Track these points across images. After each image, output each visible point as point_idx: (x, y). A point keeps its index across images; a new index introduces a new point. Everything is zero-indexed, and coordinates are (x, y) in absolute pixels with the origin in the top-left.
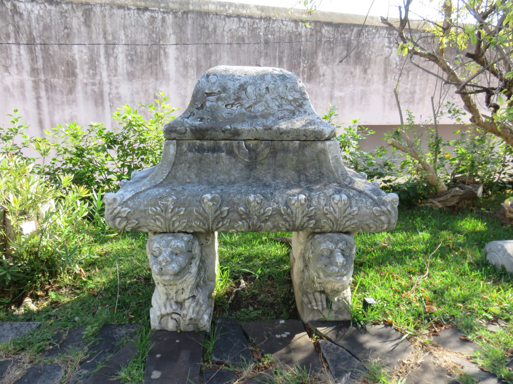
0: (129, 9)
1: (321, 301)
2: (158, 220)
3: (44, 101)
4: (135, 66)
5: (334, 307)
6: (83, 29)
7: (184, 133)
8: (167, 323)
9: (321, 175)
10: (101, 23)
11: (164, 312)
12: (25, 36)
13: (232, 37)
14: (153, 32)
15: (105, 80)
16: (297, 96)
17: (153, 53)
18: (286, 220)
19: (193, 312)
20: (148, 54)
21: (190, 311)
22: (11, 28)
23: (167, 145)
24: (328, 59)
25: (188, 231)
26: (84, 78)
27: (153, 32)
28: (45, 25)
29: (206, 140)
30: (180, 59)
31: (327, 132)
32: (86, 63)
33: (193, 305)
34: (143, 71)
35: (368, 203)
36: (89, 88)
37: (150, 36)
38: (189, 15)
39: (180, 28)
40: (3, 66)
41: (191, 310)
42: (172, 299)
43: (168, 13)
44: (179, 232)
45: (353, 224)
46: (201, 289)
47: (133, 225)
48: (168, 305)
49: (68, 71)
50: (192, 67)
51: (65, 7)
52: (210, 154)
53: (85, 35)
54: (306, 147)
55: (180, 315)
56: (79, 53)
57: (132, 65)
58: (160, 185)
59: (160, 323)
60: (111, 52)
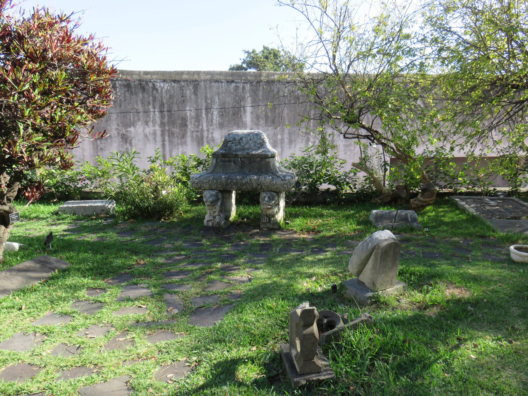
0: (222, 82)
3: (167, 143)
5: (271, 222)
9: (267, 171)
11: (208, 219)
12: (158, 102)
14: (237, 96)
15: (205, 128)
16: (261, 141)
21: (217, 219)
22: (151, 98)
26: (192, 127)
27: (237, 96)
28: (170, 95)
31: (270, 154)
34: (229, 123)
36: (195, 134)
37: (235, 99)
38: (261, 84)
39: (254, 92)
40: (145, 121)
43: (246, 83)
50: (262, 118)
51: (183, 83)
56: (190, 112)
57: (222, 118)
58: (210, 173)
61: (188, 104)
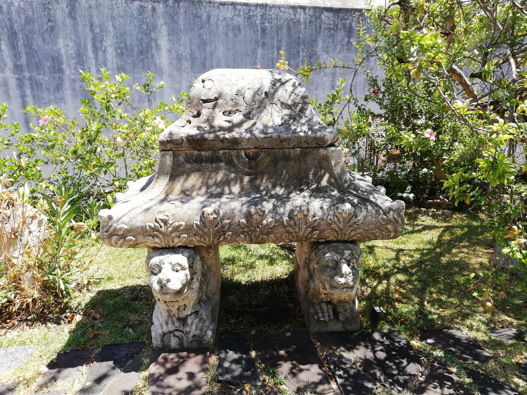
1: (328, 312)
2: (157, 236)
4: (125, 59)
5: (341, 317)
6: (68, 21)
7: (181, 144)
8: (170, 340)
10: (86, 14)
11: (165, 329)
13: (227, 26)
14: (143, 22)
17: (144, 45)
18: (289, 233)
19: (196, 329)
20: (138, 46)
23: (163, 156)
24: (328, 47)
25: (189, 246)
26: (71, 73)
28: (26, 18)
29: (204, 150)
30: (173, 51)
32: (73, 58)
33: (196, 321)
34: (134, 65)
41: (194, 327)
42: (174, 315)
44: (179, 247)
45: (358, 234)
46: (204, 303)
48: (170, 322)
49: (54, 67)
50: (186, 59)
52: (208, 164)
53: (70, 27)
54: (308, 154)
55: (182, 332)
56: (64, 46)
59: (162, 341)
60: (100, 45)
61: (61, 33)
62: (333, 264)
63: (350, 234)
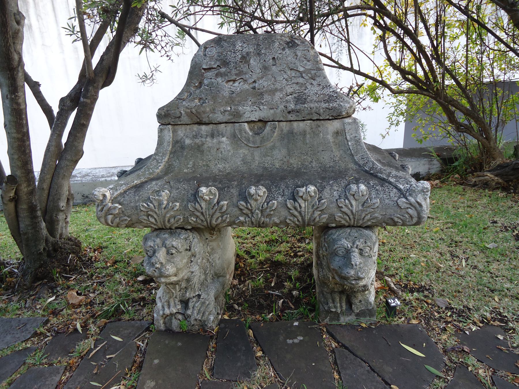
2: (152, 216)
7: (180, 117)
16: (309, 66)
25: (186, 227)
35: (392, 194)
44: (177, 228)
45: (373, 219)
47: (126, 222)
62: (343, 252)
63: (363, 219)
